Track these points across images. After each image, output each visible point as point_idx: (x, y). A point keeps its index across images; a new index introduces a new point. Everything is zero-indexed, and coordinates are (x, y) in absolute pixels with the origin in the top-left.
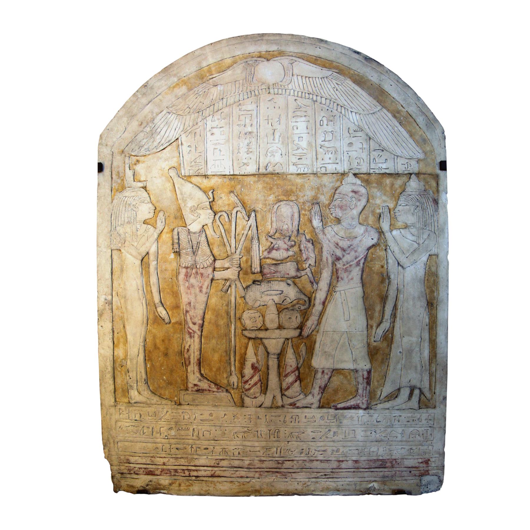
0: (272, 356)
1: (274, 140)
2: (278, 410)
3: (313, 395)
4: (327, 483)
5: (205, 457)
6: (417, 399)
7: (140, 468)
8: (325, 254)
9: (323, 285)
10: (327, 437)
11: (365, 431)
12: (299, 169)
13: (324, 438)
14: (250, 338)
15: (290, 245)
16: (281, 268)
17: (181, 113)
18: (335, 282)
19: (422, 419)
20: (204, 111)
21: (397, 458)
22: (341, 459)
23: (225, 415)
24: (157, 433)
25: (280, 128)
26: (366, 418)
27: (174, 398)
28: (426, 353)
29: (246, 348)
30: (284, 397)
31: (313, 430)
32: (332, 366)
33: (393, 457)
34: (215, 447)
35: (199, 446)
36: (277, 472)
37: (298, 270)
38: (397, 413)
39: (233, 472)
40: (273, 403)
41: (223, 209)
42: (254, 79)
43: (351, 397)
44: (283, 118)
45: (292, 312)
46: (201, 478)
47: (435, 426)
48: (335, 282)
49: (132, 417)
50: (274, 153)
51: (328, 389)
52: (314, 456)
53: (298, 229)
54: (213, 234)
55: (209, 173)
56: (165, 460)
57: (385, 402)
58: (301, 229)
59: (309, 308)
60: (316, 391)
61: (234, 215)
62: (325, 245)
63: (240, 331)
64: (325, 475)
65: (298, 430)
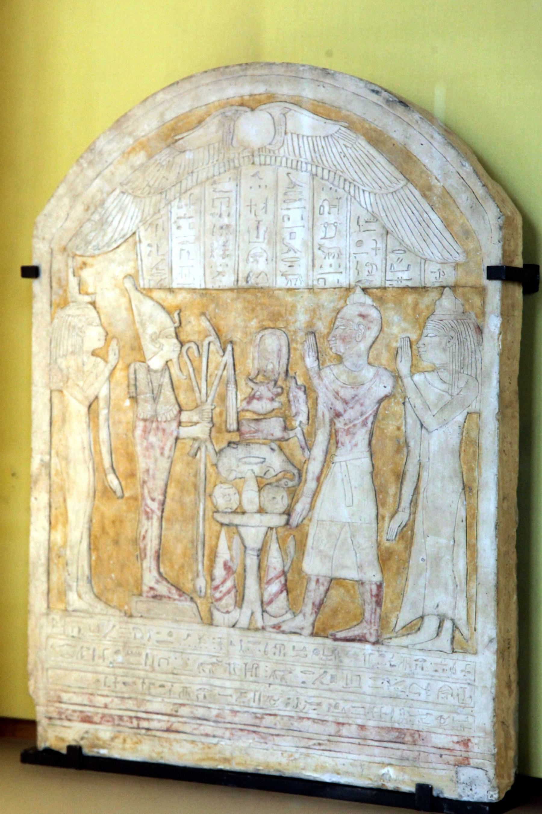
0: (250, 552)
1: (257, 237)
2: (257, 633)
3: (304, 615)
4: (322, 758)
5: (159, 699)
6: (449, 637)
7: (75, 711)
8: (322, 408)
9: (318, 452)
10: (322, 683)
11: (375, 679)
12: (289, 283)
13: (318, 683)
14: (222, 525)
16: (263, 425)
18: (333, 448)
19: (457, 669)
21: (421, 729)
22: (341, 720)
23: (188, 635)
24: (100, 657)
25: (266, 219)
26: (375, 658)
27: (124, 607)
28: (461, 565)
29: (218, 538)
30: (265, 614)
31: (303, 669)
32: (329, 573)
33: (415, 728)
34: (175, 685)
35: (153, 681)
36: (254, 732)
37: (285, 429)
38: (420, 655)
39: (196, 726)
40: (250, 623)
42: (235, 140)
43: (355, 623)
44: (271, 203)
45: (276, 489)
46: (154, 733)
47: (476, 684)
48: (333, 448)
49: (69, 631)
50: (258, 258)
51: (325, 607)
52: (304, 711)
53: (287, 370)
54: (178, 371)
56: (108, 700)
57: (403, 635)
58: (292, 369)
59: (299, 484)
60: (308, 609)
62: (321, 395)
63: (211, 514)
64: (320, 744)
65: (282, 667)
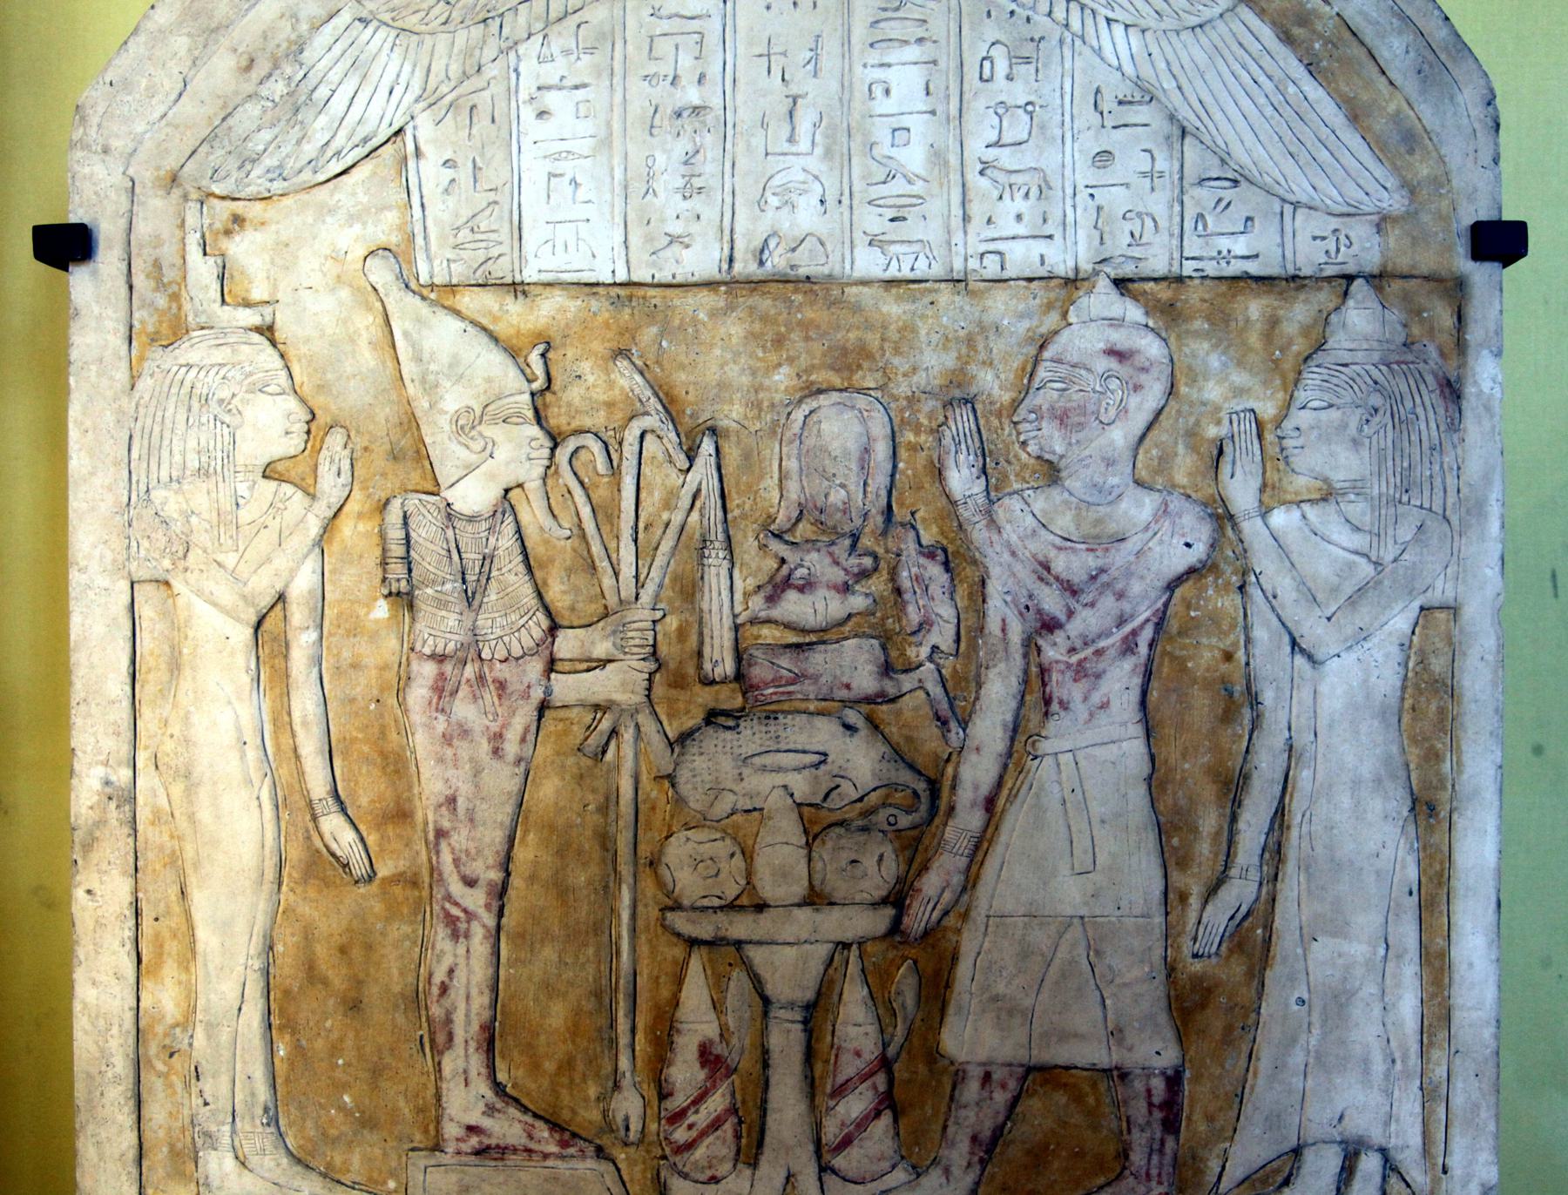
15: (856, 570)
17: (412, 21)
20: (508, 17)
41: (587, 422)
55: (530, 274)
58: (902, 505)
61: (630, 450)
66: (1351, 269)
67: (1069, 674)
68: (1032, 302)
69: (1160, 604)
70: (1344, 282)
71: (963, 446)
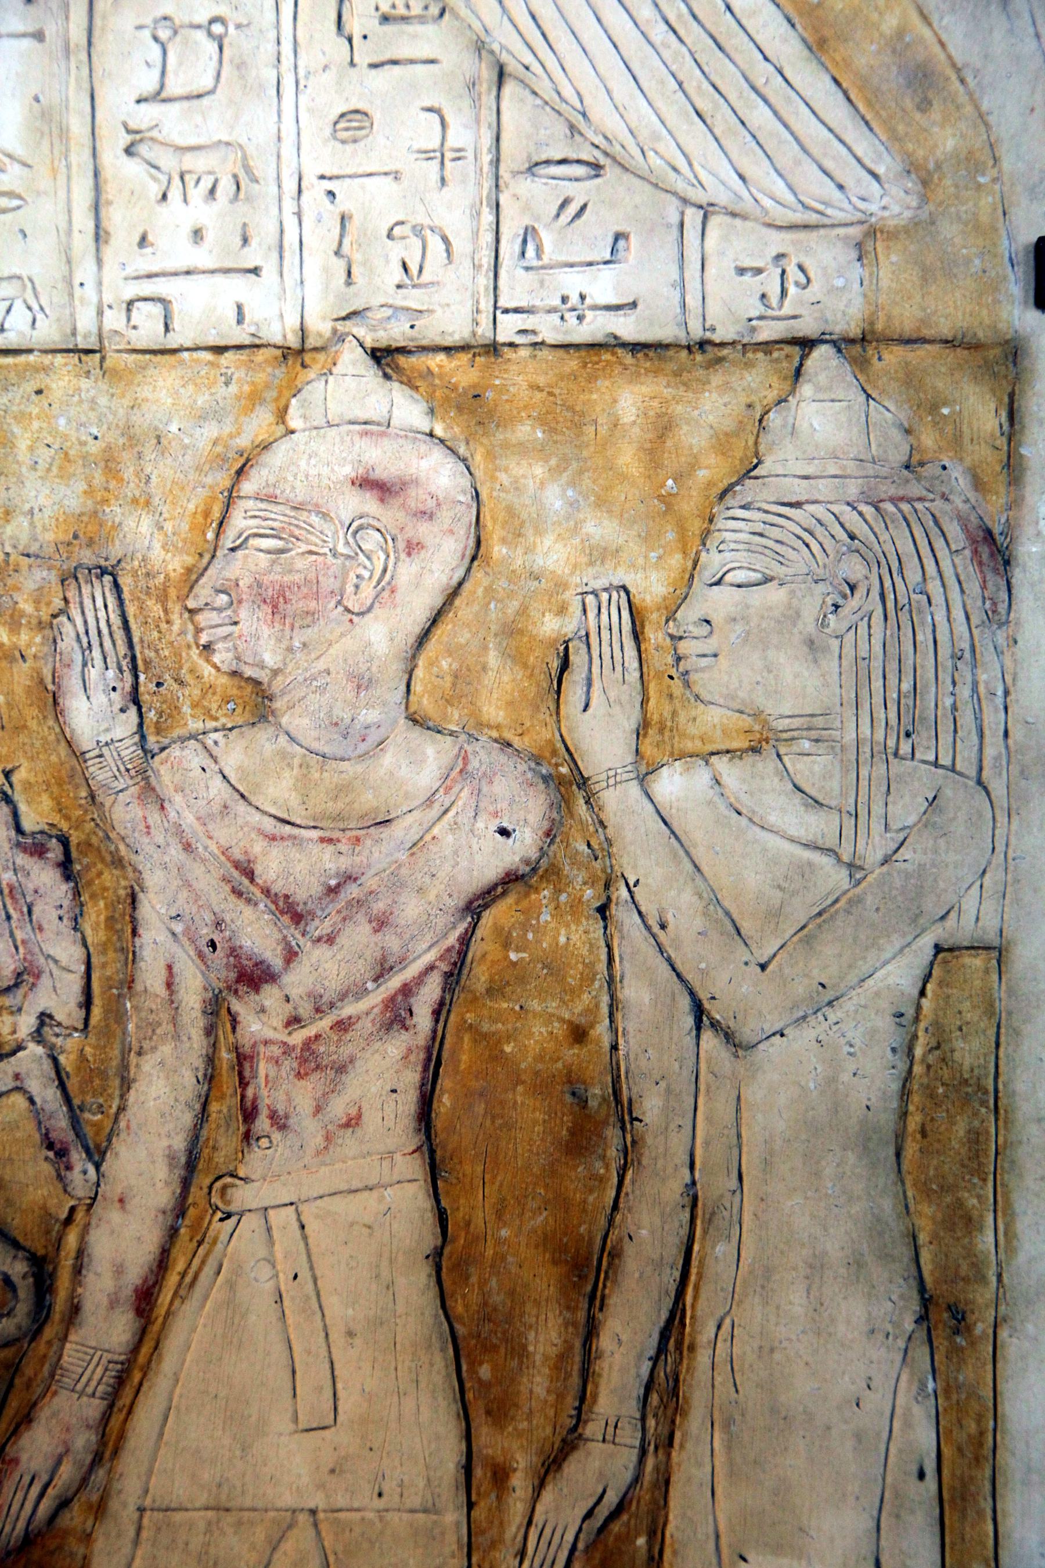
66: (807, 327)
67: (289, 1065)
68: (221, 391)
69: (452, 939)
70: (796, 351)
71: (96, 653)
